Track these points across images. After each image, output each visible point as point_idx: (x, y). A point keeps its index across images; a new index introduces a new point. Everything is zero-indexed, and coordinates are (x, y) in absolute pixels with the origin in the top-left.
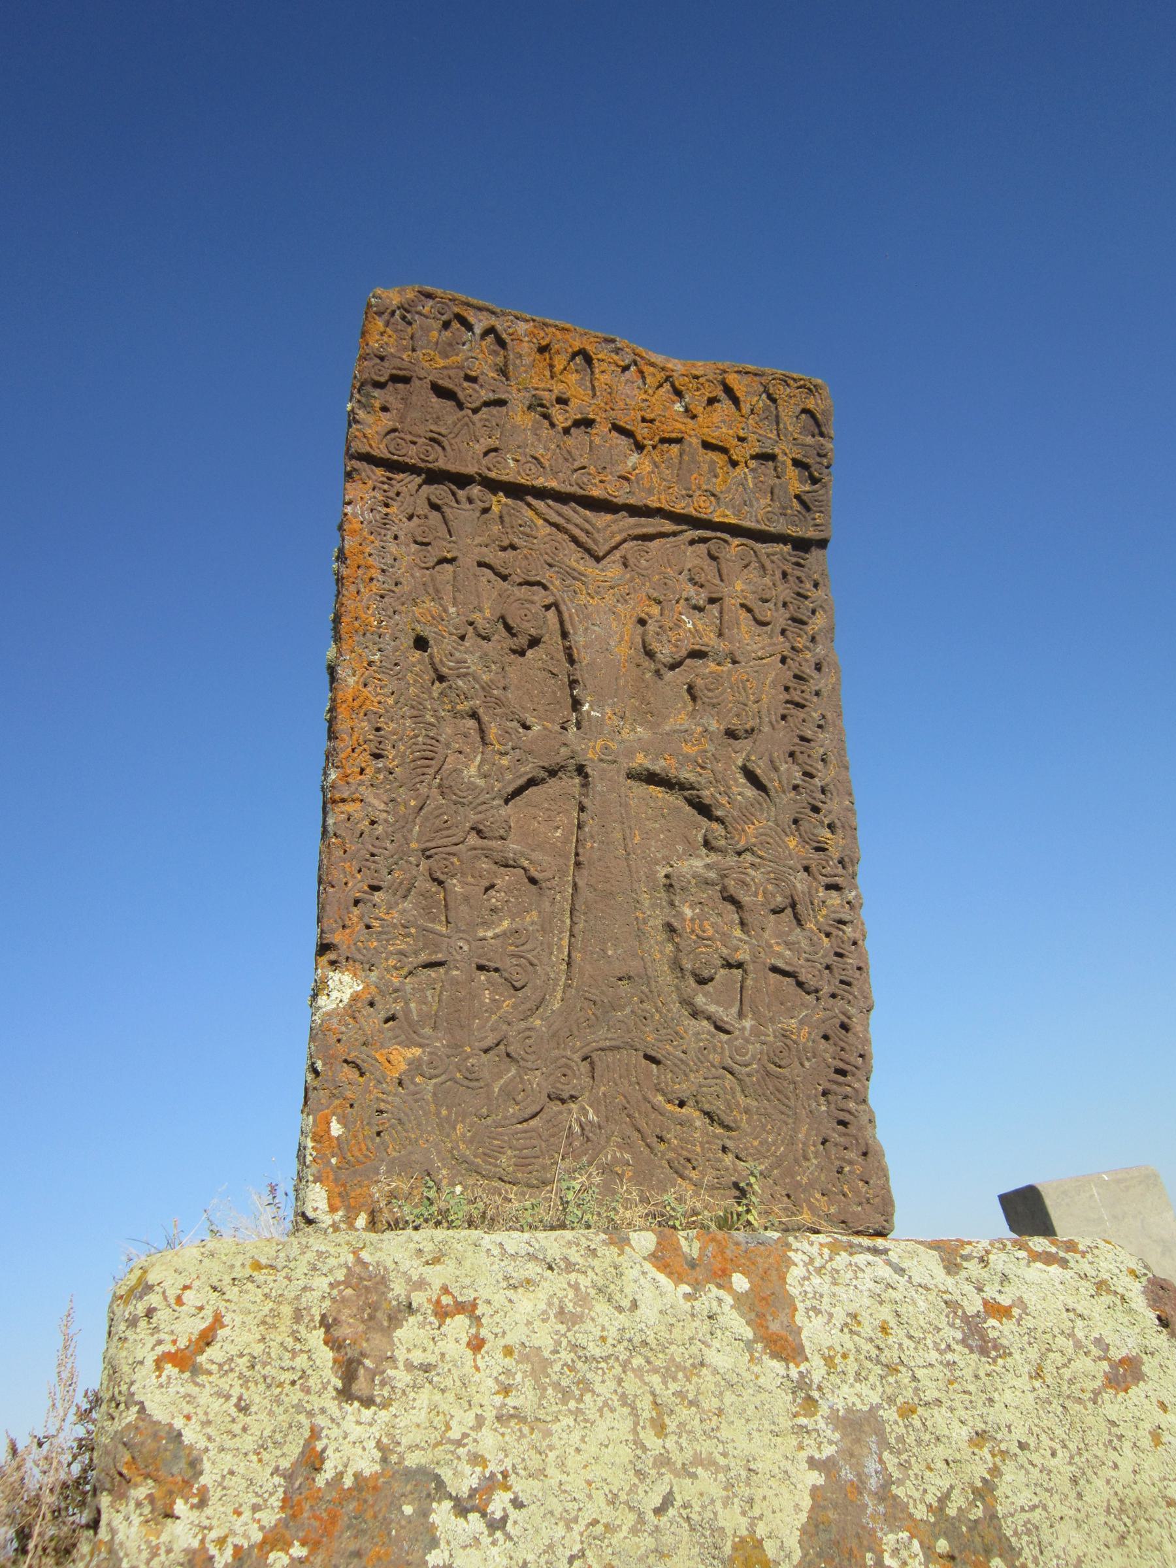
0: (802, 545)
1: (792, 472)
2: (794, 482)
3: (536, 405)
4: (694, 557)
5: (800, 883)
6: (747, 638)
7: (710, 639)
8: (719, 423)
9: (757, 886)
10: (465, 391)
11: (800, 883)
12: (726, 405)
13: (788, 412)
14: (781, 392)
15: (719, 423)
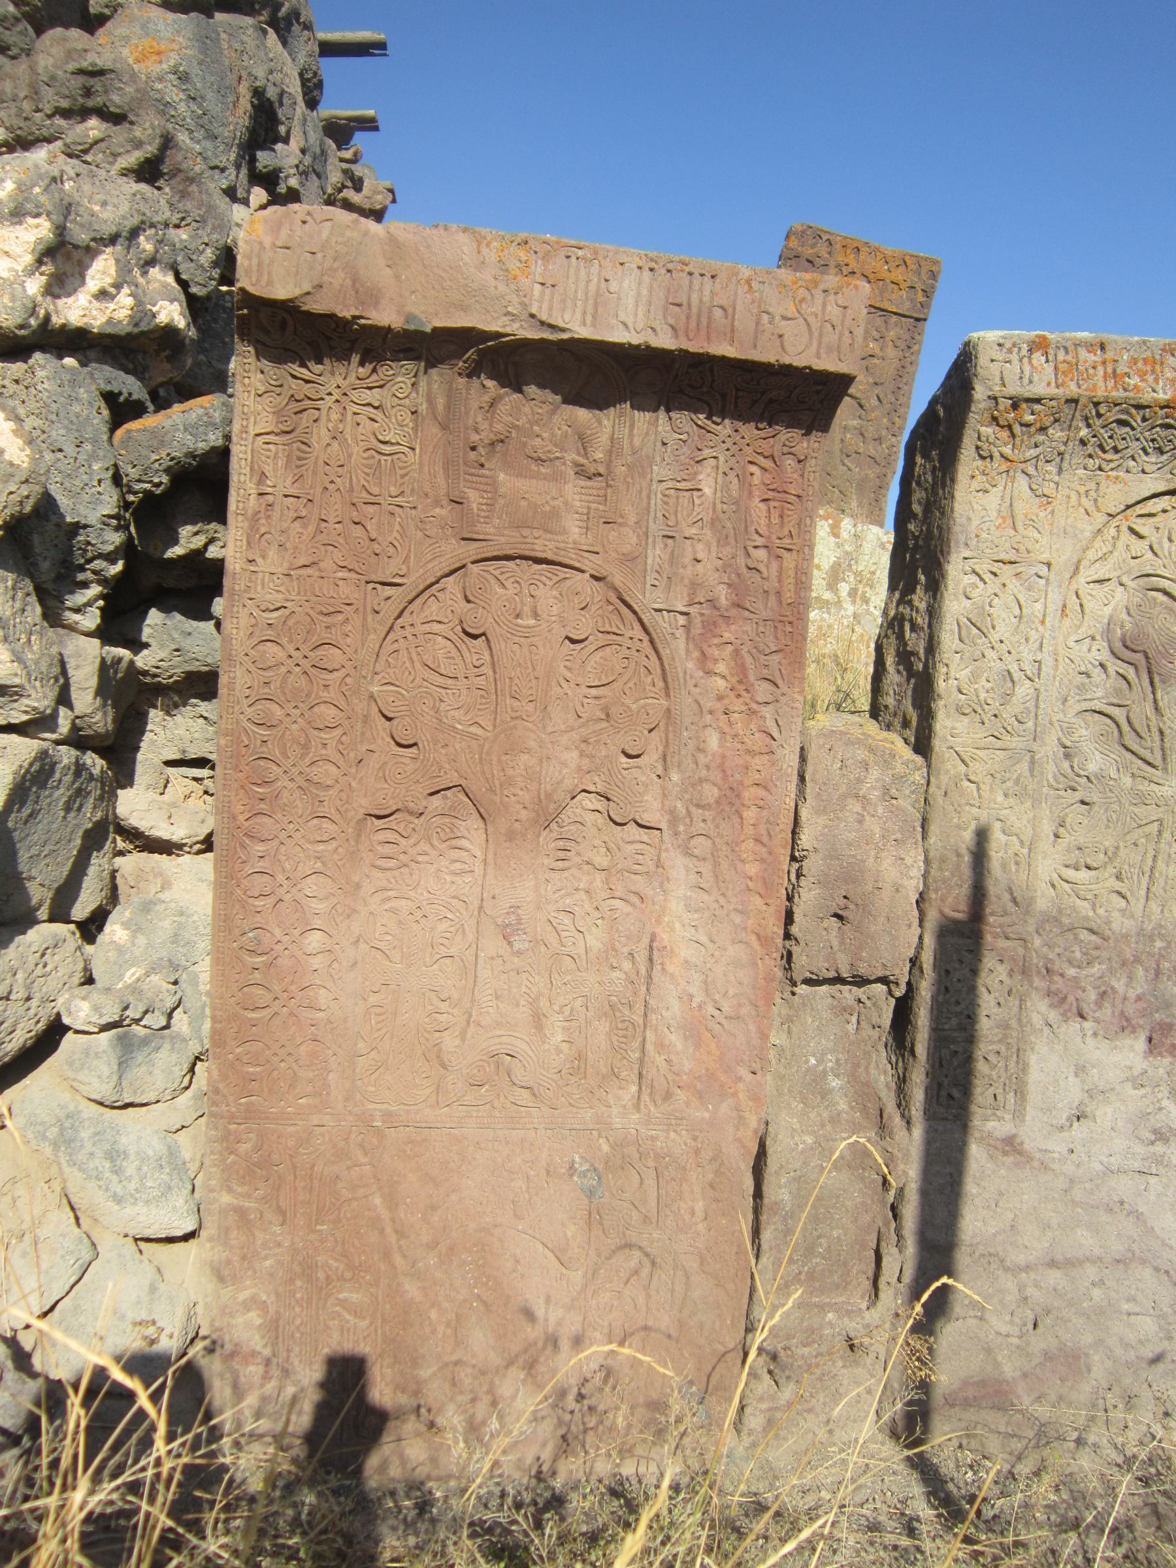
0: (918, 320)
1: (920, 293)
2: (920, 297)
3: (838, 266)
4: (879, 321)
5: (884, 432)
6: (891, 352)
7: (877, 351)
8: (898, 275)
9: (871, 432)
10: (817, 261)
11: (884, 432)
12: (903, 268)
13: (924, 271)
14: (923, 263)
15: (898, 275)
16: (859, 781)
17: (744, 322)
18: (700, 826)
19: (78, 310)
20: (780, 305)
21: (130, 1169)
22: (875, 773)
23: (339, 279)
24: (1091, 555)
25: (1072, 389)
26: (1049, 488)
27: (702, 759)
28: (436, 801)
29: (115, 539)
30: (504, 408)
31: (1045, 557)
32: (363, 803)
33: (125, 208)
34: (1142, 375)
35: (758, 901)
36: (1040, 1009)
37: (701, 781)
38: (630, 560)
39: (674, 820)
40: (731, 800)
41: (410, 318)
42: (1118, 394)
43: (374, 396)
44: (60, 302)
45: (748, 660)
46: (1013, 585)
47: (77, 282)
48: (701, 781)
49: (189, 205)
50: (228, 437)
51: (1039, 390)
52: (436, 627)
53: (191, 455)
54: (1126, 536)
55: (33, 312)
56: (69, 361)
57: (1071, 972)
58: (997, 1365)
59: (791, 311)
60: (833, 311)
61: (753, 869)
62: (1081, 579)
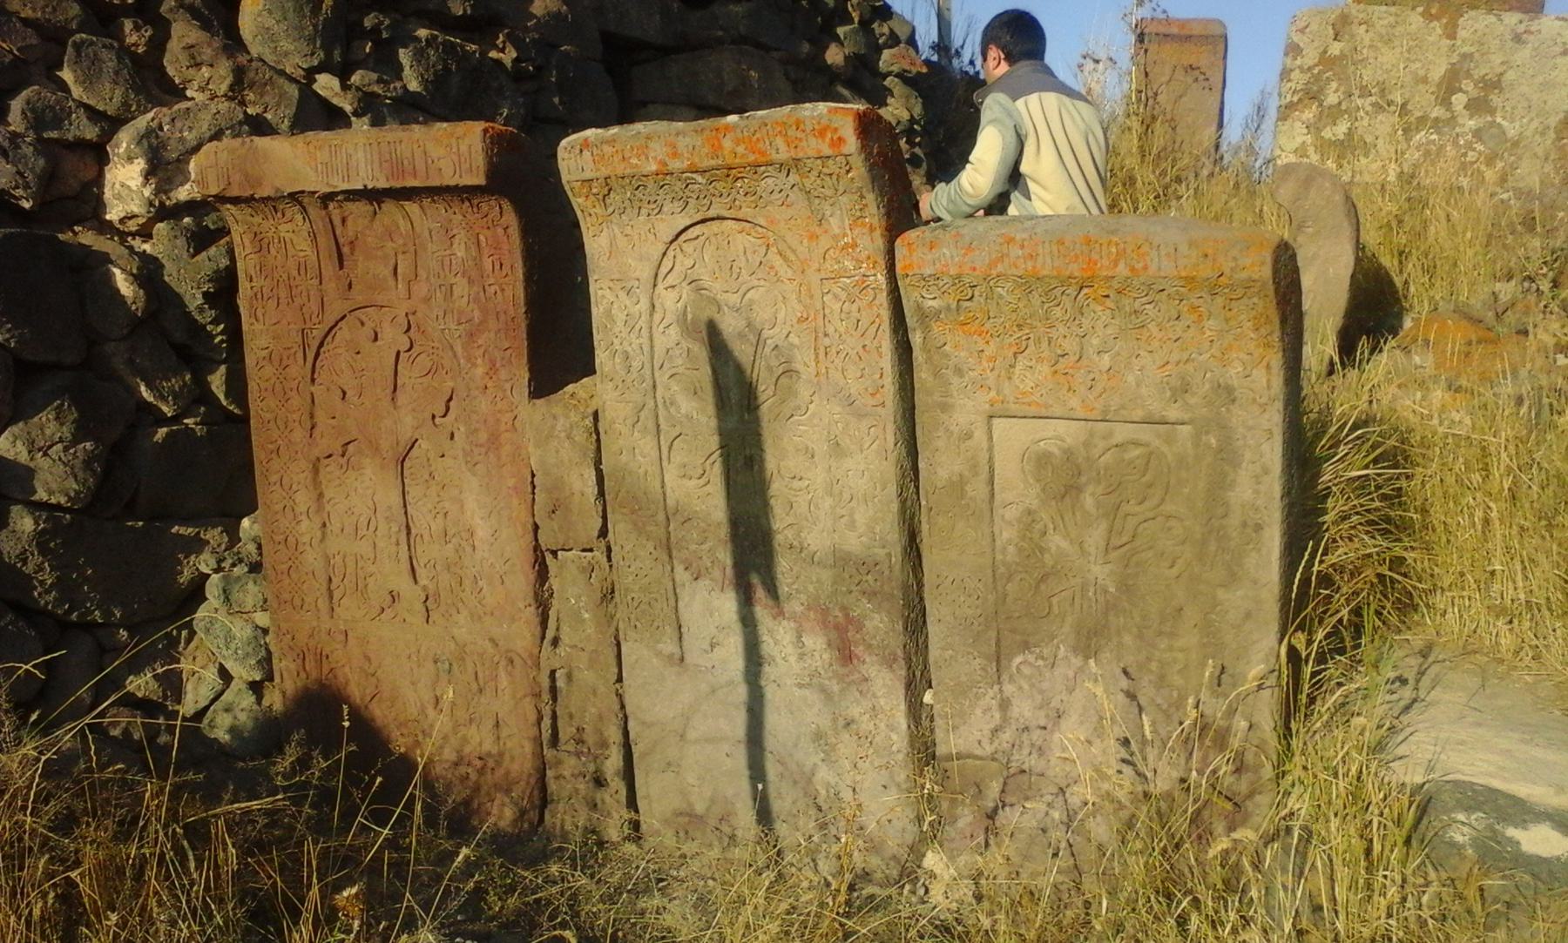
16: (553, 427)
17: (420, 165)
18: (477, 458)
19: (183, 193)
20: (436, 151)
21: (233, 646)
22: (562, 420)
23: (237, 178)
24: (664, 270)
25: (604, 172)
26: (628, 230)
27: (475, 417)
28: (350, 447)
29: (210, 314)
30: (349, 222)
31: (637, 274)
32: (316, 452)
33: (205, 127)
34: (638, 157)
35: (515, 502)
36: (681, 575)
37: (476, 430)
38: (427, 300)
39: (466, 454)
40: (494, 440)
41: (278, 190)
42: (628, 171)
43: (289, 226)
44: (172, 194)
45: (498, 355)
46: (622, 294)
47: (181, 178)
48: (476, 430)
49: (267, 98)
50: (233, 259)
51: (588, 175)
52: (339, 351)
53: (217, 272)
54: (680, 257)
55: (151, 204)
56: (187, 220)
57: (693, 547)
58: (690, 805)
59: (442, 152)
60: (464, 148)
61: (511, 482)
62: (660, 286)
